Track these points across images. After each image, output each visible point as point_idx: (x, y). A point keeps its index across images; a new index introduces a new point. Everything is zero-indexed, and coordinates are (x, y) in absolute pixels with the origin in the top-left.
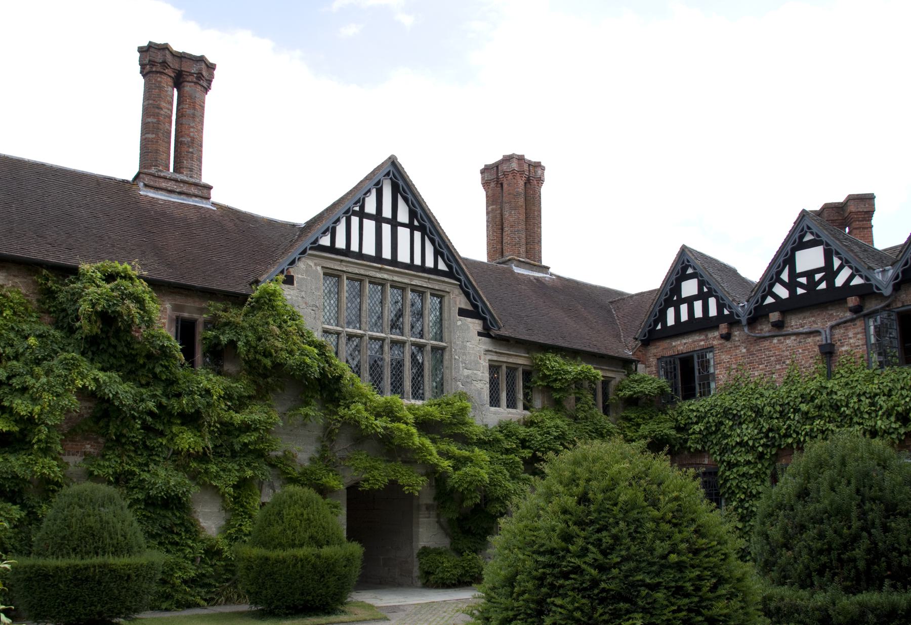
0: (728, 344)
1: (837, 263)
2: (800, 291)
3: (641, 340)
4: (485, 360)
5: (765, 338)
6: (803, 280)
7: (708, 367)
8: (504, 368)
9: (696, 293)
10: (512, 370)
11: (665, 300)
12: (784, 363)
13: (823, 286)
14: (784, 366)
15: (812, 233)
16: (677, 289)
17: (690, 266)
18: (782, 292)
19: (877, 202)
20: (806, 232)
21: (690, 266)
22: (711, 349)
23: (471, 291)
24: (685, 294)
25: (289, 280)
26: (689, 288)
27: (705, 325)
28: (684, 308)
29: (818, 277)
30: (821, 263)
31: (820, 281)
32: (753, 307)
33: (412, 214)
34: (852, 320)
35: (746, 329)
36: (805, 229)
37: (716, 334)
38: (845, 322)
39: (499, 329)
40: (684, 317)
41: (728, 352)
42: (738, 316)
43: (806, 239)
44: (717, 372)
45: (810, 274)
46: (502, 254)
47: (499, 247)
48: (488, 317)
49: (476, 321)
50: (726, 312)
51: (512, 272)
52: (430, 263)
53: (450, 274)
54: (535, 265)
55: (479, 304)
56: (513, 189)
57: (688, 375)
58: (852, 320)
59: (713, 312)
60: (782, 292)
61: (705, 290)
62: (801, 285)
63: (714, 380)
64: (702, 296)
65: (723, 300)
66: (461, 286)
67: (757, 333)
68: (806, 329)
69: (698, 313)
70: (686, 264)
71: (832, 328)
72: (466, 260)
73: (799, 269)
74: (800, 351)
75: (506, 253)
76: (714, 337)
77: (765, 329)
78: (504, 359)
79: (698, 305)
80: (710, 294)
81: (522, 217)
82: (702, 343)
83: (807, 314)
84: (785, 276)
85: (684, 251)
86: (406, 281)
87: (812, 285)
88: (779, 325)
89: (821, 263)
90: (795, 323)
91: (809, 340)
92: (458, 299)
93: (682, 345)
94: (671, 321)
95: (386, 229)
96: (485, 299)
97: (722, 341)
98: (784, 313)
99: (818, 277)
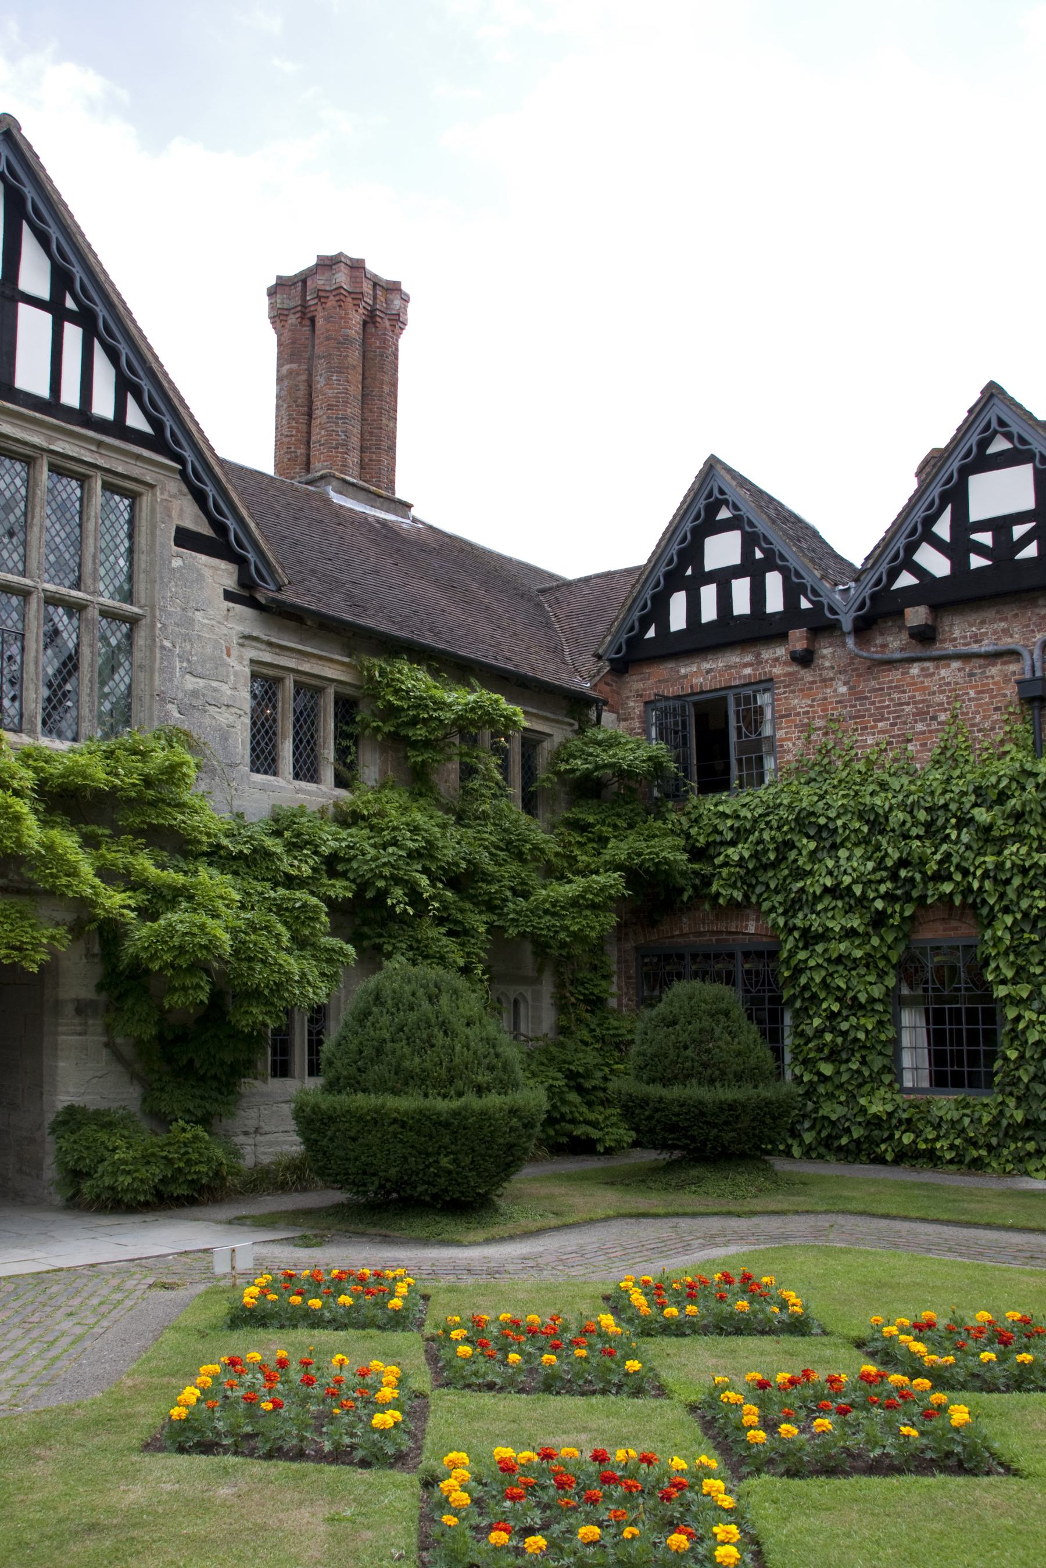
0: (807, 675)
2: (977, 562)
3: (611, 661)
4: (240, 659)
5: (890, 663)
6: (985, 538)
7: (758, 724)
8: (289, 684)
9: (736, 560)
10: (309, 689)
11: (668, 575)
12: (934, 718)
13: (1031, 551)
14: (935, 726)
15: (1008, 436)
16: (693, 552)
17: (726, 502)
18: (937, 564)
20: (995, 432)
21: (726, 502)
22: (767, 683)
23: (210, 490)
26: (722, 550)
27: (757, 631)
28: (709, 594)
31: (1025, 540)
32: (868, 592)
35: (850, 642)
36: (994, 424)
37: (781, 651)
39: (279, 589)
40: (709, 613)
41: (806, 691)
42: (833, 611)
43: (992, 449)
44: (780, 734)
45: (1000, 525)
46: (308, 467)
47: (301, 451)
48: (251, 556)
49: (223, 564)
50: (805, 604)
51: (328, 501)
53: (157, 442)
54: (379, 496)
55: (231, 523)
56: (338, 330)
57: (714, 742)
59: (775, 603)
60: (937, 564)
61: (759, 555)
62: (981, 549)
63: (772, 751)
64: (752, 569)
65: (798, 575)
66: (183, 473)
67: (874, 652)
68: (986, 646)
69: (741, 605)
70: (715, 499)
72: (222, 462)
73: (977, 513)
74: (972, 694)
75: (316, 465)
76: (774, 659)
77: (895, 643)
78: (291, 663)
79: (741, 589)
80: (771, 562)
81: (355, 390)
82: (748, 671)
83: (990, 614)
85: (712, 466)
86: (36, 439)
87: (1004, 548)
88: (925, 636)
90: (961, 632)
91: (994, 670)
92: (176, 505)
93: (702, 674)
94: (678, 621)
96: (244, 513)
97: (794, 668)
98: (937, 608)
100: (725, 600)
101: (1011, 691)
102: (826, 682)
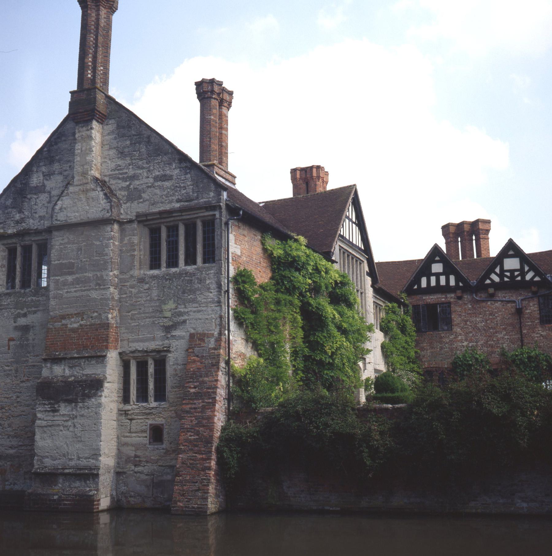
0: (460, 302)
1: (526, 268)
2: (506, 279)
5: (483, 301)
6: (508, 274)
9: (441, 270)
14: (494, 317)
18: (496, 279)
19: (492, 224)
24: (433, 271)
26: (437, 268)
27: (447, 289)
28: (433, 279)
29: (516, 273)
30: (518, 267)
31: (518, 276)
34: (532, 298)
37: (453, 295)
38: (528, 298)
40: (433, 283)
45: (512, 271)
58: (532, 298)
60: (496, 279)
62: (507, 277)
68: (507, 299)
71: (522, 300)
76: (451, 297)
82: (443, 299)
84: (497, 270)
87: (512, 277)
88: (492, 296)
89: (518, 267)
90: (500, 295)
91: (509, 305)
93: (431, 299)
98: (496, 289)
99: (516, 273)
100: (438, 281)
101: (513, 310)
102: (465, 304)
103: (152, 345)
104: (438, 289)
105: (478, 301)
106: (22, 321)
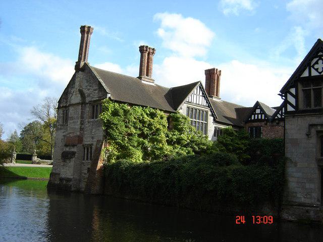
16: (255, 111)
18: (279, 116)
22: (262, 126)
25: (181, 109)
27: (261, 120)
28: (256, 116)
33: (203, 93)
37: (263, 123)
40: (256, 118)
52: (205, 105)
53: (209, 107)
59: (263, 118)
60: (279, 116)
69: (260, 118)
70: (258, 105)
79: (260, 115)
84: (280, 113)
88: (278, 124)
93: (255, 124)
94: (253, 118)
95: (198, 97)
100: (258, 117)
103: (89, 143)
104: (258, 120)
105: (273, 126)
106: (64, 134)
